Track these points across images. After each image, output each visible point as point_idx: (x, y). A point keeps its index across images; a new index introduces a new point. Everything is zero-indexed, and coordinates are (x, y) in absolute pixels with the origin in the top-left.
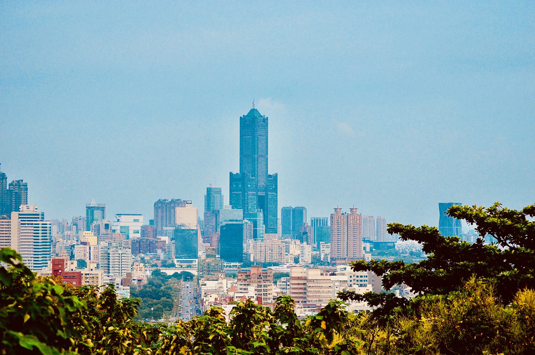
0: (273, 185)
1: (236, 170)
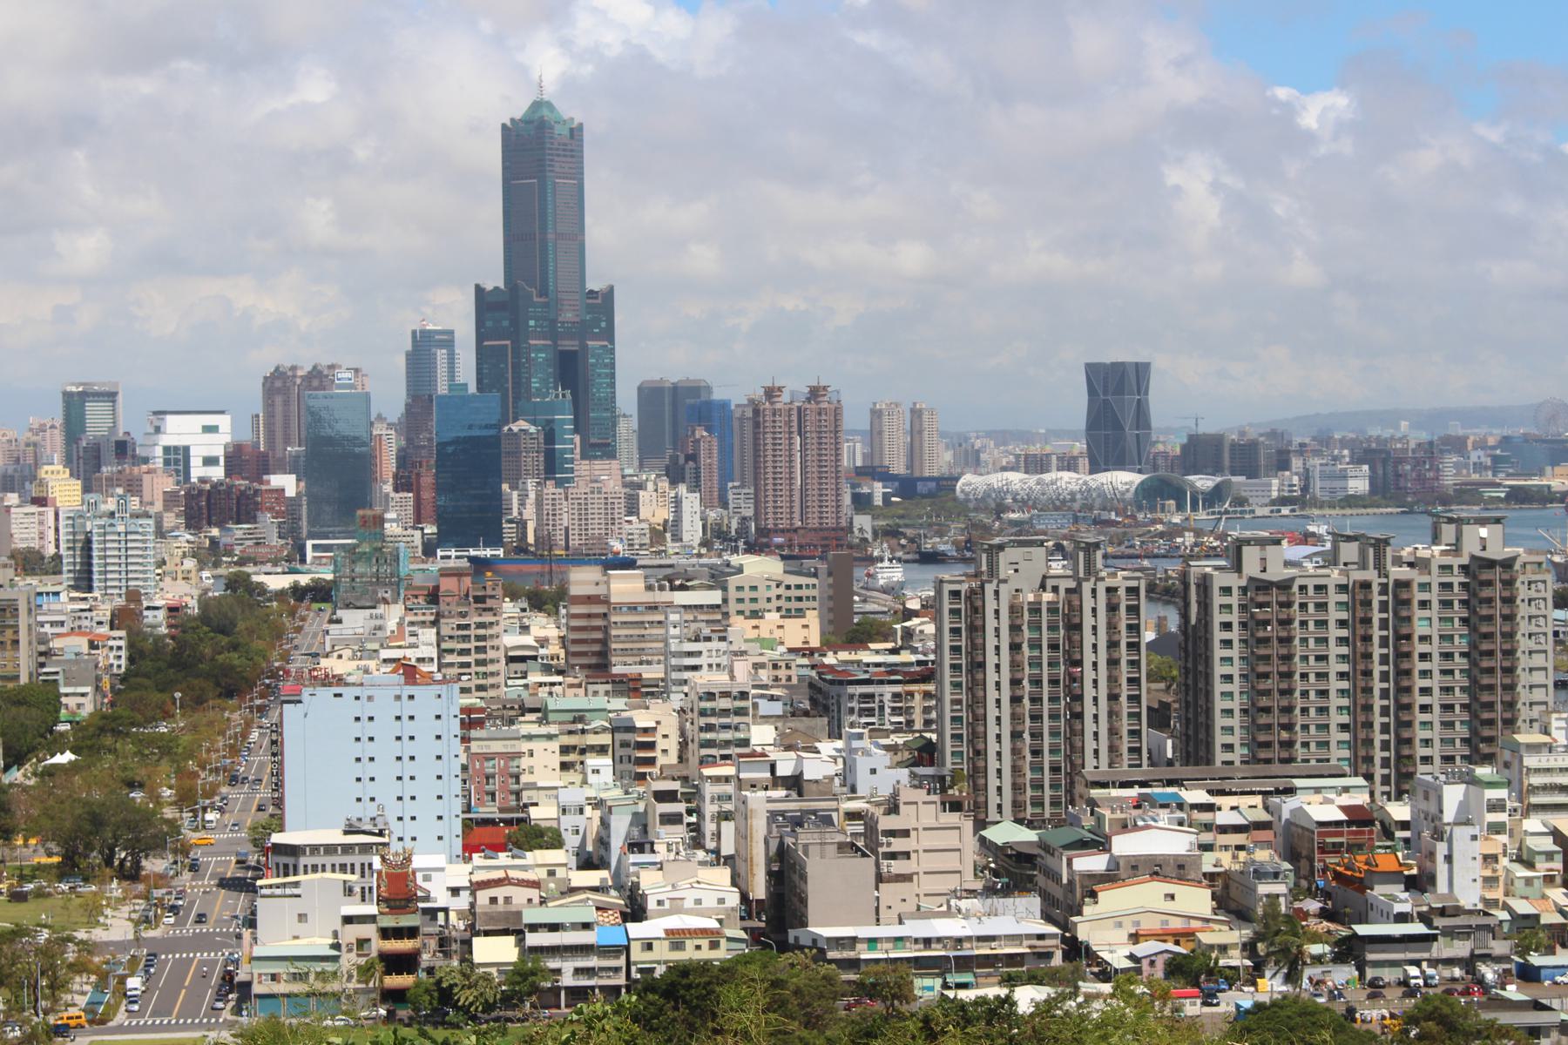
1: (494, 279)
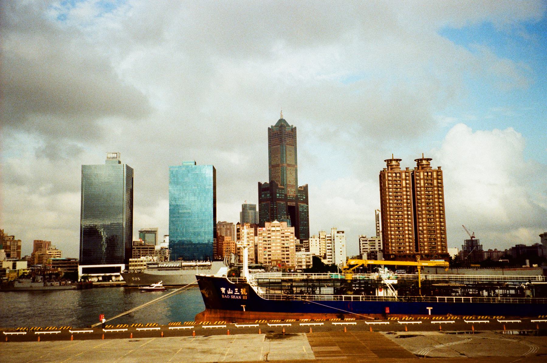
0: (303, 196)
1: (266, 180)
